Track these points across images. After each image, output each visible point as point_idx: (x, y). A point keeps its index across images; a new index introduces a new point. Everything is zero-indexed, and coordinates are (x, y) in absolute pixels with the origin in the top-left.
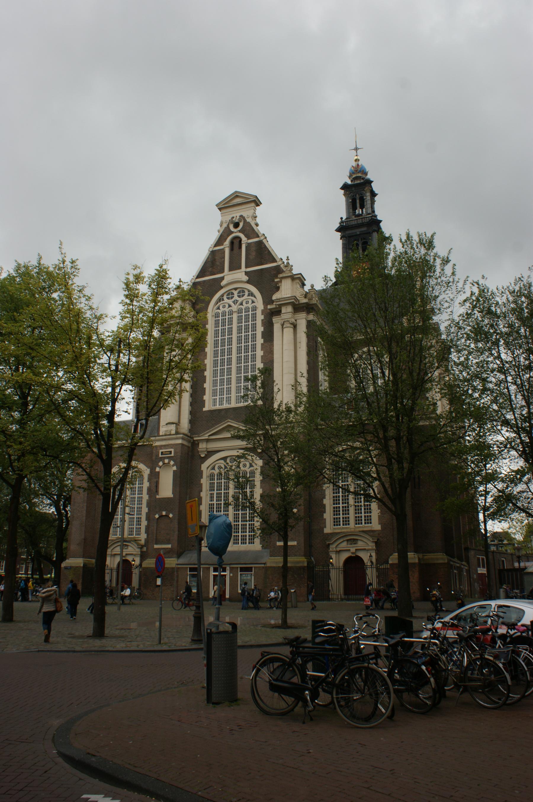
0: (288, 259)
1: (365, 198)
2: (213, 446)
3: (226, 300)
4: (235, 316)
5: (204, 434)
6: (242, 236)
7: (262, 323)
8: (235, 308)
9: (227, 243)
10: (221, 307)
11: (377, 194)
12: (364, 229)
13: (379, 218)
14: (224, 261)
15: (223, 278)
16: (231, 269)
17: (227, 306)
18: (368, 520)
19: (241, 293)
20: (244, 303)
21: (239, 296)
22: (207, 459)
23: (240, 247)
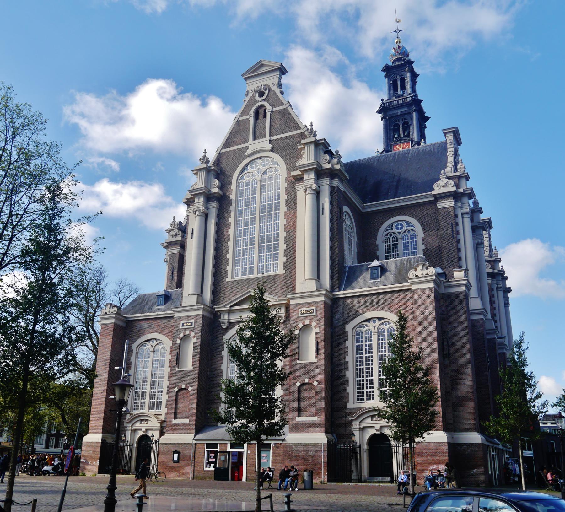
0: (312, 125)
6: (266, 104)
7: (286, 191)
9: (252, 113)
11: (419, 75)
12: (405, 109)
13: (420, 98)
15: (247, 148)
16: (255, 138)
22: (229, 330)
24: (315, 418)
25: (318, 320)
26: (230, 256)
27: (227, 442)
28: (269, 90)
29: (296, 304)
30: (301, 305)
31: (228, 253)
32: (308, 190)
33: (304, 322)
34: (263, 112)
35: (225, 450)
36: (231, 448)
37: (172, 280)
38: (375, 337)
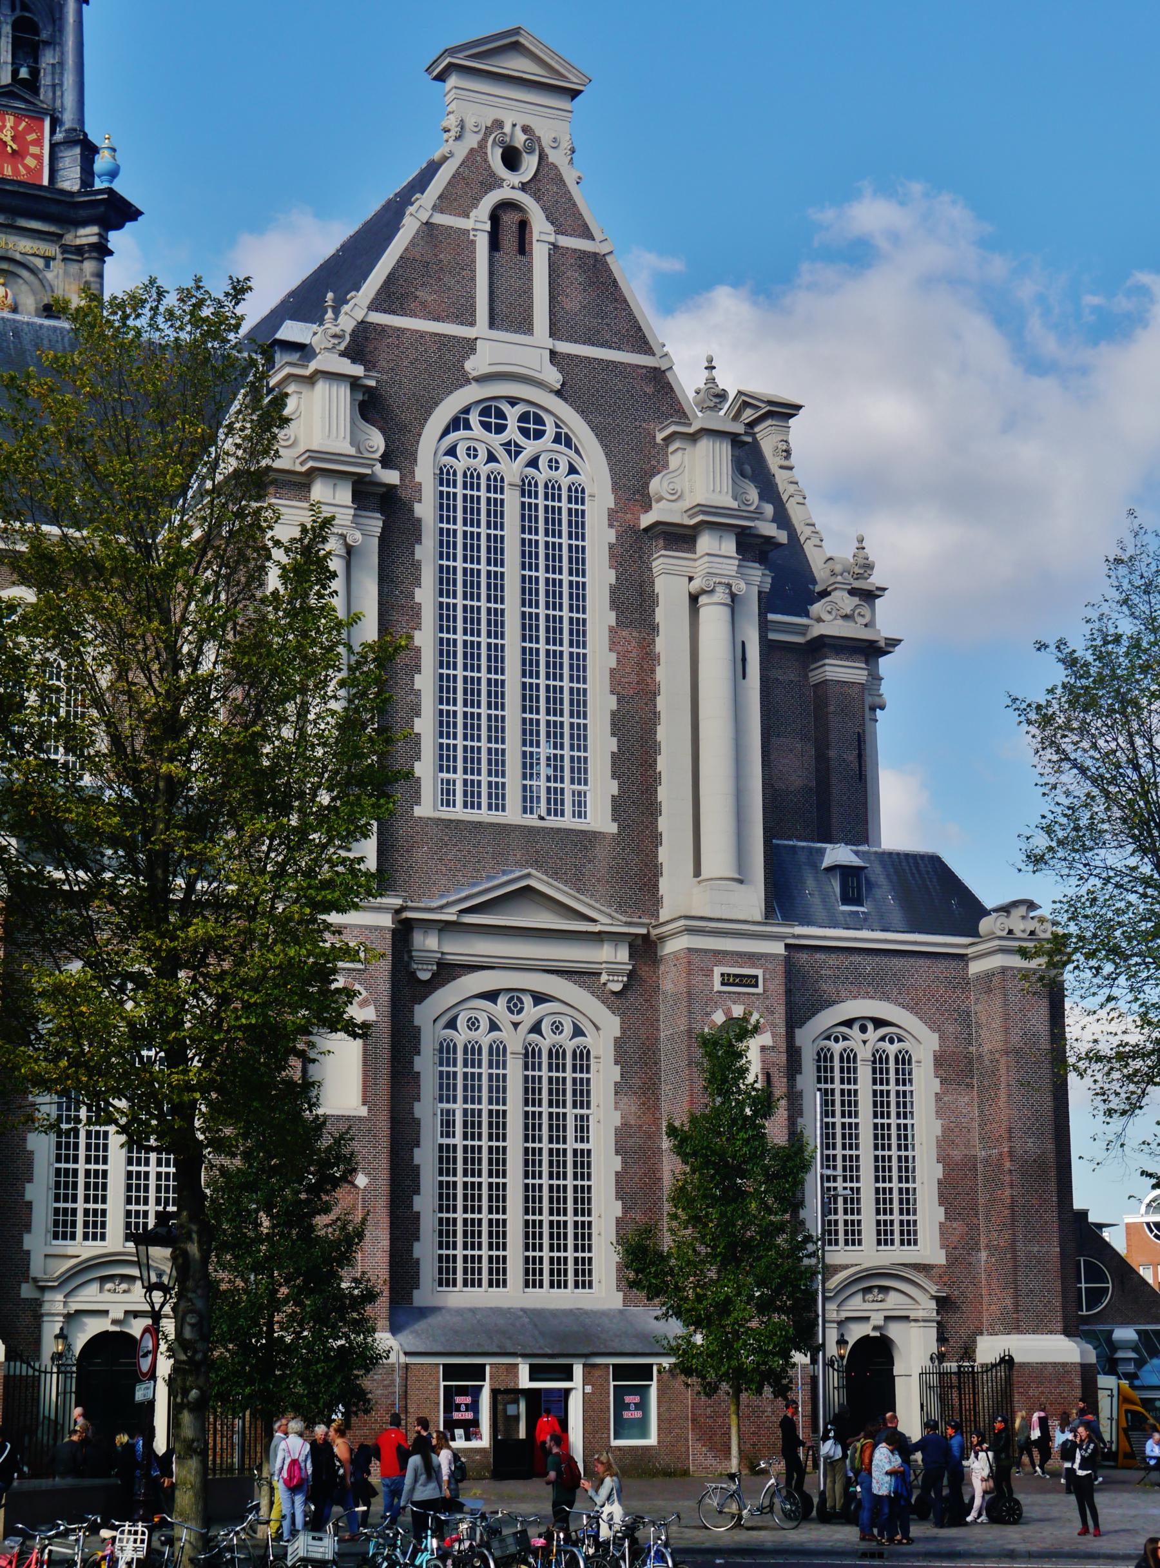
2: (458, 949)
3: (478, 431)
4: (512, 501)
5: (448, 905)
8: (511, 470)
10: (461, 450)
15: (469, 346)
17: (483, 455)
18: (909, 1237)
19: (532, 424)
20: (543, 462)
21: (525, 432)
22: (436, 989)
23: (523, 248)
25: (767, 1008)
26: (425, 726)
27: (519, 1360)
28: (542, 157)
29: (706, 951)
30: (720, 956)
31: (418, 715)
32: (720, 589)
33: (729, 1009)
34: (515, 228)
35: (511, 1386)
36: (531, 1379)
38: (864, 1073)
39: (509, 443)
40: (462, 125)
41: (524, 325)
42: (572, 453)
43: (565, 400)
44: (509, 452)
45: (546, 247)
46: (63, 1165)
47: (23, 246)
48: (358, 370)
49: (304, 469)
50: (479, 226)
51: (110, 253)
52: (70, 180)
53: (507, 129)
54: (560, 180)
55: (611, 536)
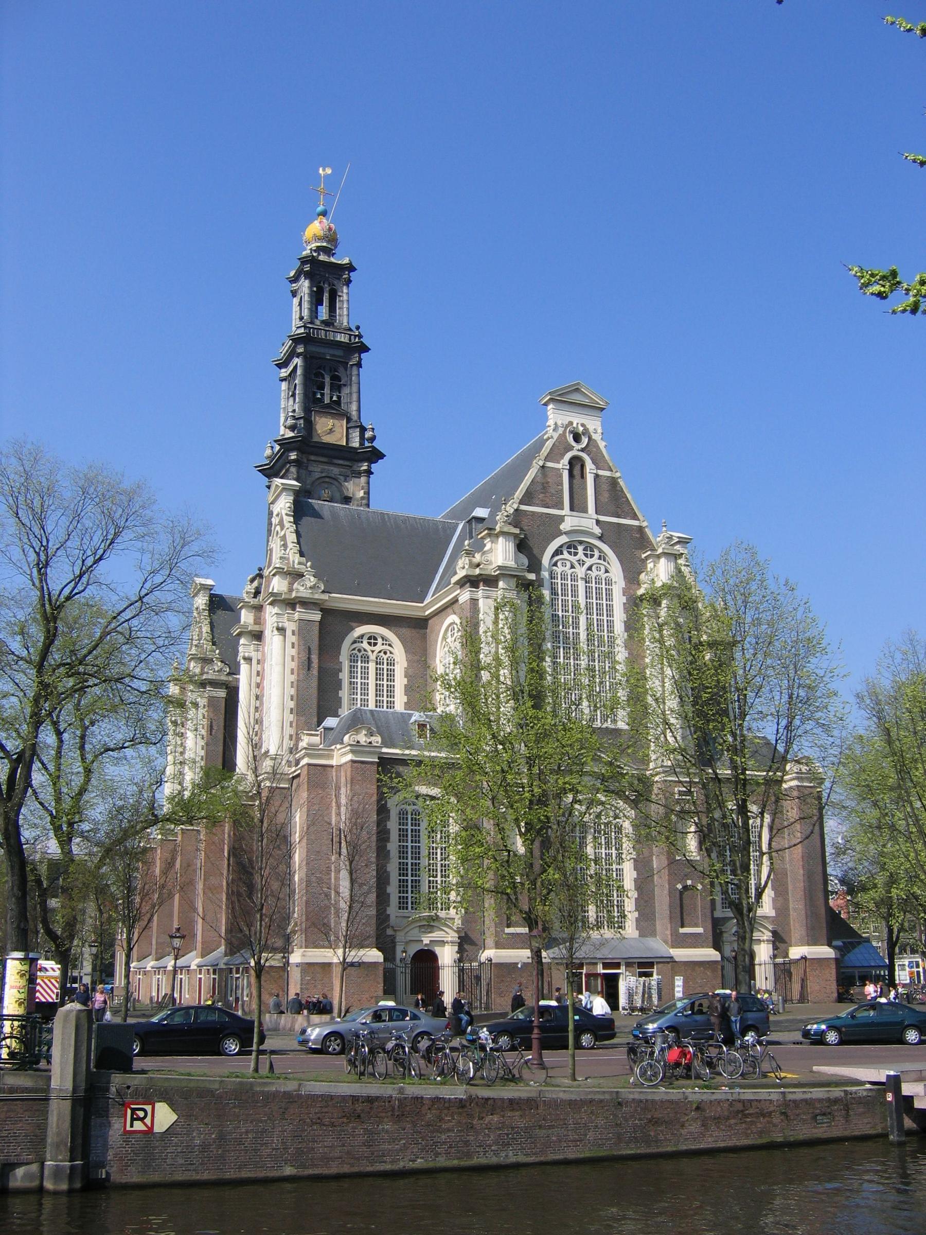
1: (340, 294)
4: (581, 585)
8: (581, 571)
10: (559, 564)
14: (562, 490)
15: (561, 519)
17: (568, 565)
21: (586, 555)
23: (583, 476)
24: (700, 930)
28: (590, 438)
35: (595, 972)
36: (604, 969)
37: (309, 669)
39: (579, 560)
40: (556, 424)
41: (584, 510)
42: (606, 564)
43: (603, 541)
44: (580, 564)
45: (593, 475)
46: (402, 878)
47: (335, 471)
48: (517, 531)
49: (496, 573)
50: (564, 467)
51: (372, 473)
52: (355, 443)
53: (575, 425)
54: (597, 447)
55: (624, 600)
